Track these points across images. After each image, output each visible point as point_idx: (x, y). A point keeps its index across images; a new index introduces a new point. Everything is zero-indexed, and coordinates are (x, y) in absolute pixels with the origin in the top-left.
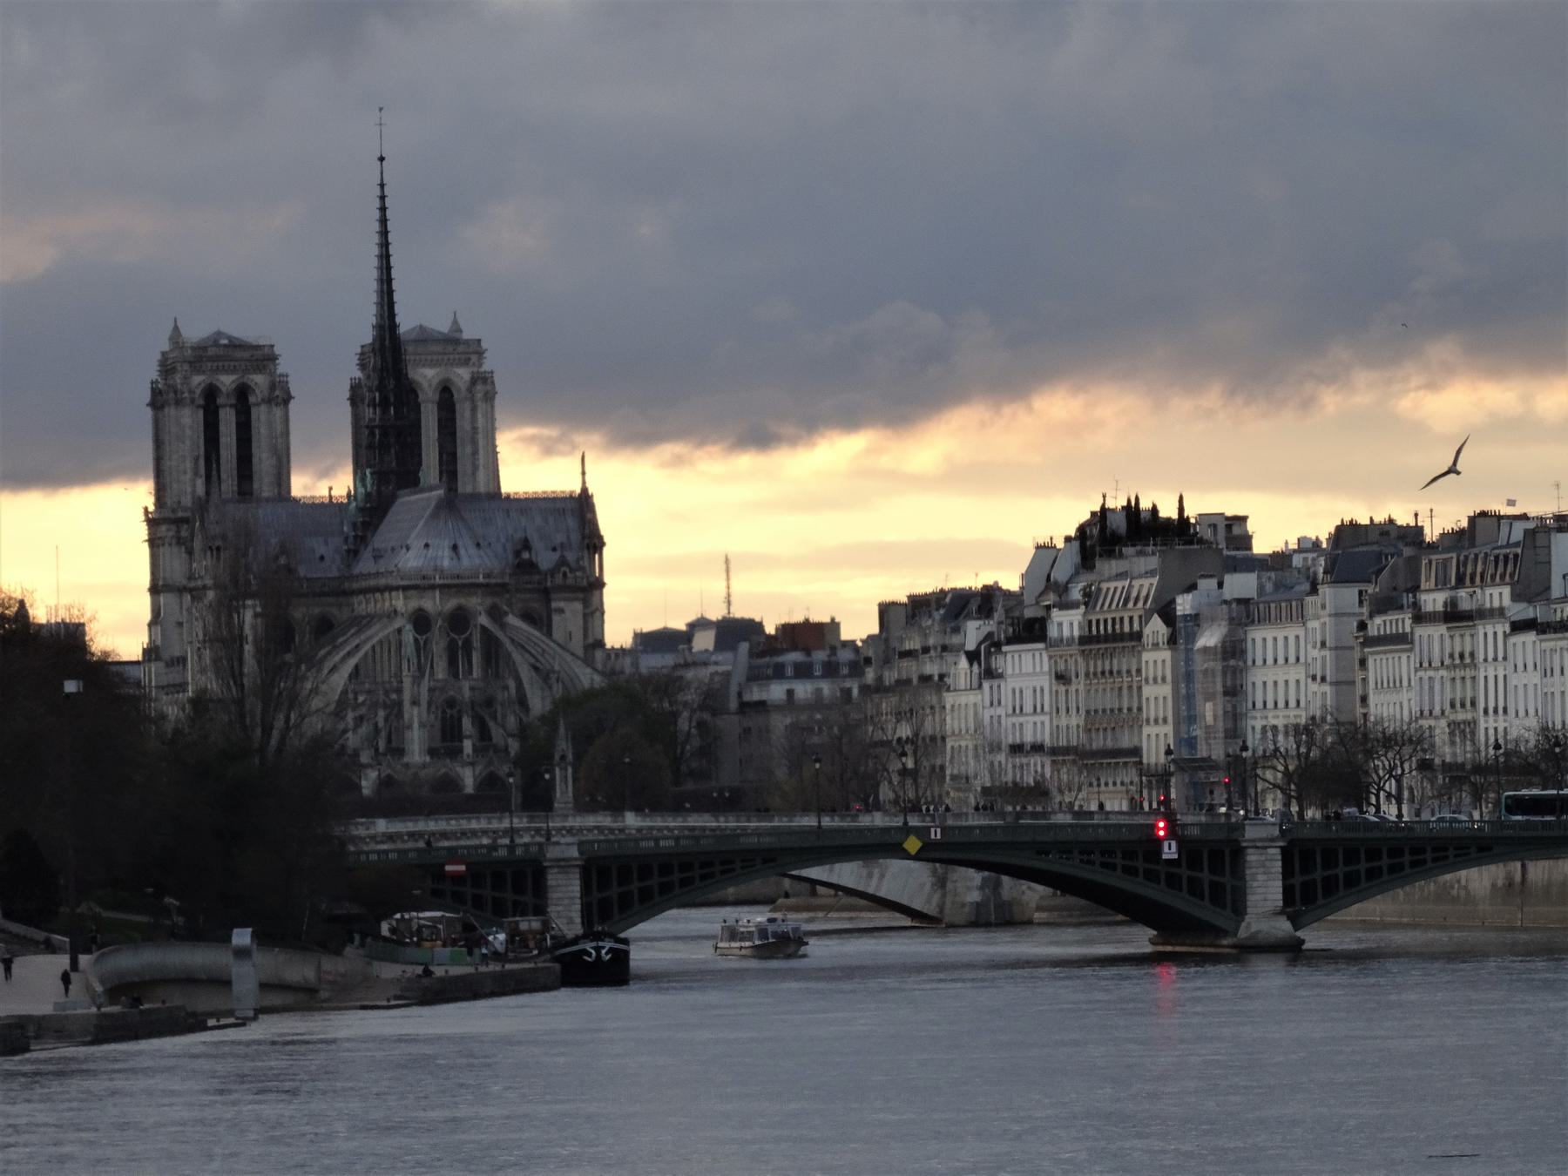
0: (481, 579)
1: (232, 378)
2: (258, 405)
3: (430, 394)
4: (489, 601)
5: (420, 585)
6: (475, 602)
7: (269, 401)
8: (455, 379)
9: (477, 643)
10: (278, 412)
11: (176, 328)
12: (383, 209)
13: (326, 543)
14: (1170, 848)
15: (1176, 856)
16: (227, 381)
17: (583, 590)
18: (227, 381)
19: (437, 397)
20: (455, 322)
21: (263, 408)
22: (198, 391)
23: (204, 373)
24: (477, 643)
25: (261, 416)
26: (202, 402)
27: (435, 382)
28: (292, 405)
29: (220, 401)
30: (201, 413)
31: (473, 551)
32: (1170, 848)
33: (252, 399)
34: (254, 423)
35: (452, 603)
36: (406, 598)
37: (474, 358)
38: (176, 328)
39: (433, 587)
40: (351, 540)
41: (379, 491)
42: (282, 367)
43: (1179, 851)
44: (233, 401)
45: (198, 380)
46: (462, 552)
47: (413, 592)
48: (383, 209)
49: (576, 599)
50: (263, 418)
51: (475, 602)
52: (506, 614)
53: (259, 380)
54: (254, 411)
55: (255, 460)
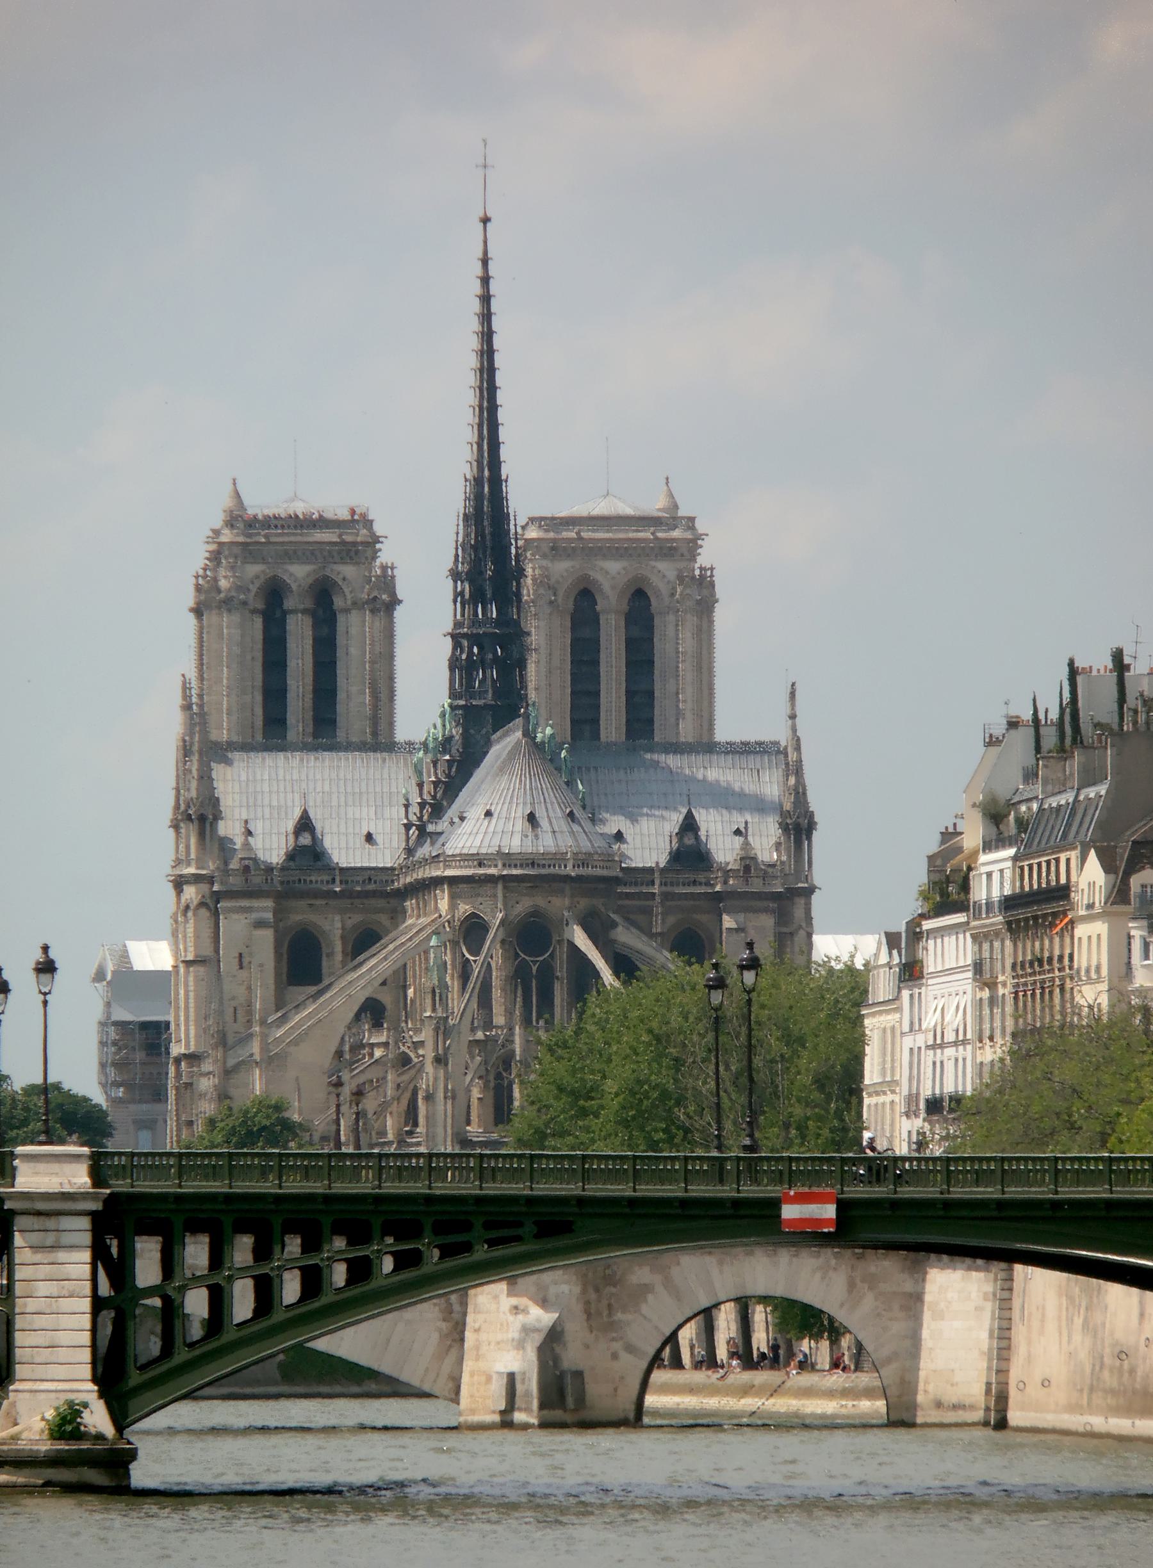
0: (570, 871)
1: (308, 568)
2: (347, 611)
4: (583, 903)
6: (558, 905)
8: (655, 581)
9: (561, 970)
12: (485, 280)
16: (299, 574)
17: (776, 896)
18: (299, 574)
22: (254, 589)
24: (561, 970)
26: (260, 606)
28: (399, 613)
29: (289, 603)
30: (259, 622)
31: (562, 824)
33: (338, 602)
34: (340, 640)
35: (524, 905)
36: (453, 897)
40: (414, 809)
44: (309, 604)
46: (544, 823)
47: (463, 886)
48: (485, 280)
49: (766, 910)
50: (353, 631)
51: (558, 905)
52: (614, 925)
53: (348, 571)
54: (341, 619)
55: (341, 696)
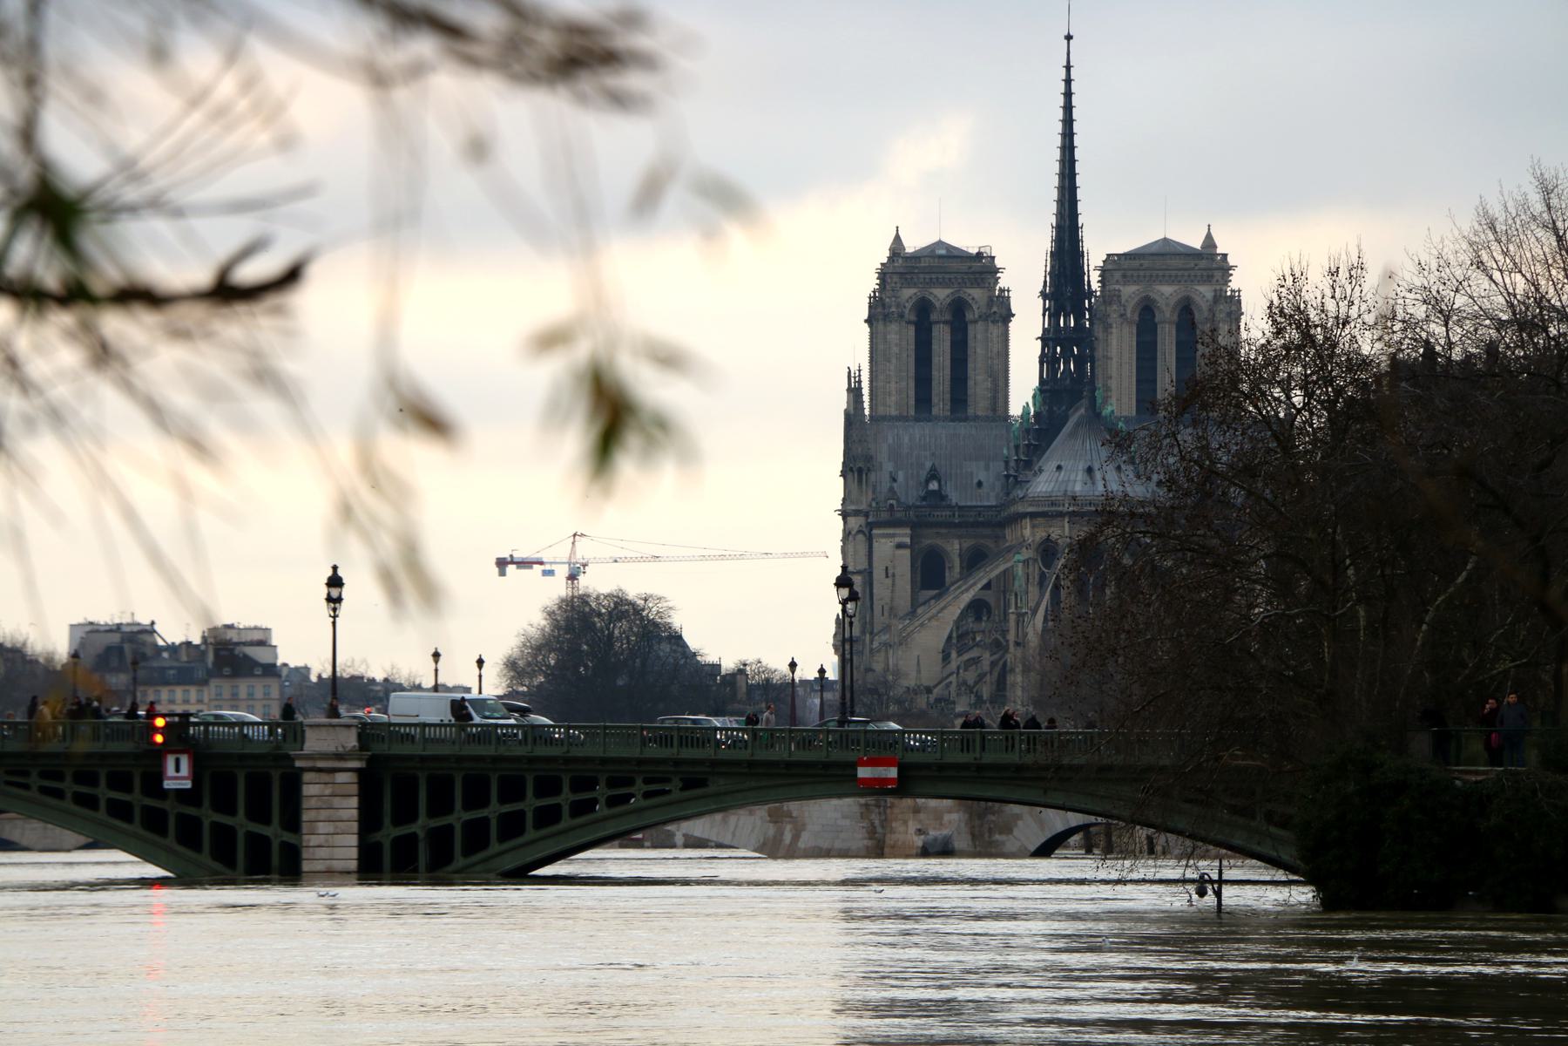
1: (948, 291)
2: (975, 322)
3: (1168, 315)
5: (1048, 513)
7: (985, 318)
8: (1197, 299)
10: (995, 330)
11: (897, 238)
13: (987, 468)
14: (178, 769)
15: (188, 785)
16: (941, 295)
18: (941, 295)
19: (1175, 318)
20: (1209, 237)
21: (980, 326)
22: (909, 306)
23: (915, 286)
25: (976, 332)
26: (913, 318)
27: (1172, 302)
29: (934, 317)
30: (912, 330)
32: (178, 769)
33: (969, 316)
34: (971, 343)
36: (1033, 527)
37: (1218, 274)
38: (897, 238)
39: (1061, 515)
41: (1050, 411)
42: (1004, 281)
43: (196, 776)
44: (948, 317)
45: (908, 293)
53: (976, 294)
54: (970, 328)
55: (970, 383)
